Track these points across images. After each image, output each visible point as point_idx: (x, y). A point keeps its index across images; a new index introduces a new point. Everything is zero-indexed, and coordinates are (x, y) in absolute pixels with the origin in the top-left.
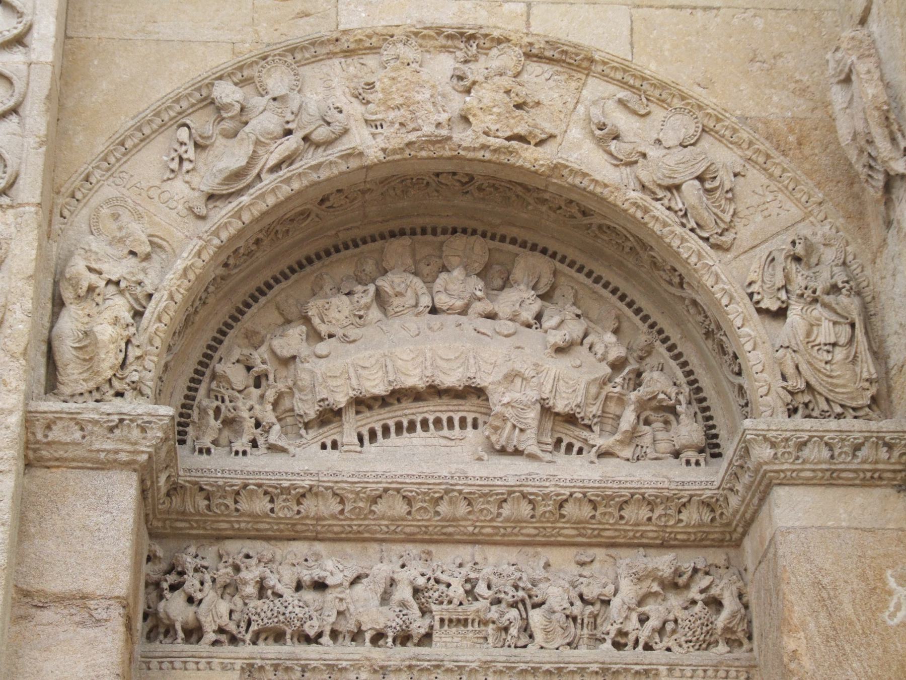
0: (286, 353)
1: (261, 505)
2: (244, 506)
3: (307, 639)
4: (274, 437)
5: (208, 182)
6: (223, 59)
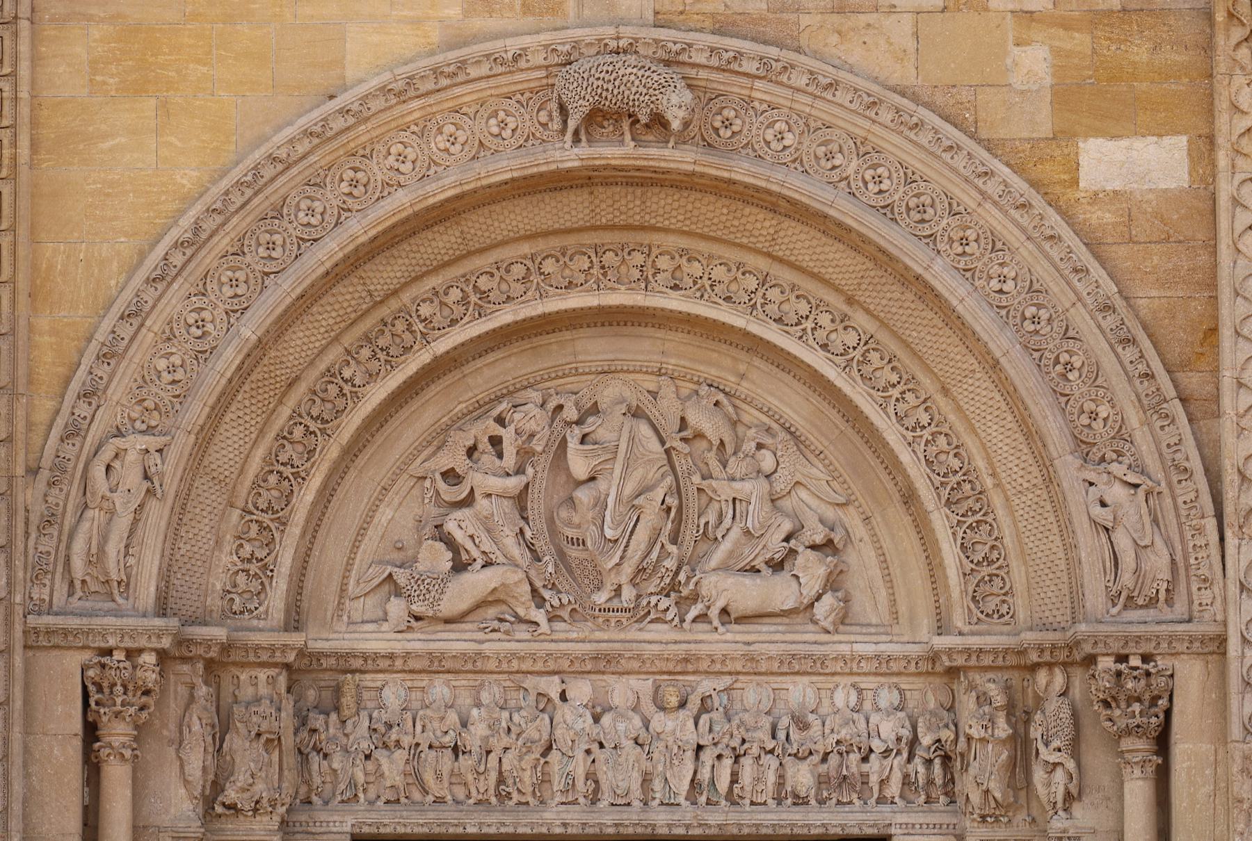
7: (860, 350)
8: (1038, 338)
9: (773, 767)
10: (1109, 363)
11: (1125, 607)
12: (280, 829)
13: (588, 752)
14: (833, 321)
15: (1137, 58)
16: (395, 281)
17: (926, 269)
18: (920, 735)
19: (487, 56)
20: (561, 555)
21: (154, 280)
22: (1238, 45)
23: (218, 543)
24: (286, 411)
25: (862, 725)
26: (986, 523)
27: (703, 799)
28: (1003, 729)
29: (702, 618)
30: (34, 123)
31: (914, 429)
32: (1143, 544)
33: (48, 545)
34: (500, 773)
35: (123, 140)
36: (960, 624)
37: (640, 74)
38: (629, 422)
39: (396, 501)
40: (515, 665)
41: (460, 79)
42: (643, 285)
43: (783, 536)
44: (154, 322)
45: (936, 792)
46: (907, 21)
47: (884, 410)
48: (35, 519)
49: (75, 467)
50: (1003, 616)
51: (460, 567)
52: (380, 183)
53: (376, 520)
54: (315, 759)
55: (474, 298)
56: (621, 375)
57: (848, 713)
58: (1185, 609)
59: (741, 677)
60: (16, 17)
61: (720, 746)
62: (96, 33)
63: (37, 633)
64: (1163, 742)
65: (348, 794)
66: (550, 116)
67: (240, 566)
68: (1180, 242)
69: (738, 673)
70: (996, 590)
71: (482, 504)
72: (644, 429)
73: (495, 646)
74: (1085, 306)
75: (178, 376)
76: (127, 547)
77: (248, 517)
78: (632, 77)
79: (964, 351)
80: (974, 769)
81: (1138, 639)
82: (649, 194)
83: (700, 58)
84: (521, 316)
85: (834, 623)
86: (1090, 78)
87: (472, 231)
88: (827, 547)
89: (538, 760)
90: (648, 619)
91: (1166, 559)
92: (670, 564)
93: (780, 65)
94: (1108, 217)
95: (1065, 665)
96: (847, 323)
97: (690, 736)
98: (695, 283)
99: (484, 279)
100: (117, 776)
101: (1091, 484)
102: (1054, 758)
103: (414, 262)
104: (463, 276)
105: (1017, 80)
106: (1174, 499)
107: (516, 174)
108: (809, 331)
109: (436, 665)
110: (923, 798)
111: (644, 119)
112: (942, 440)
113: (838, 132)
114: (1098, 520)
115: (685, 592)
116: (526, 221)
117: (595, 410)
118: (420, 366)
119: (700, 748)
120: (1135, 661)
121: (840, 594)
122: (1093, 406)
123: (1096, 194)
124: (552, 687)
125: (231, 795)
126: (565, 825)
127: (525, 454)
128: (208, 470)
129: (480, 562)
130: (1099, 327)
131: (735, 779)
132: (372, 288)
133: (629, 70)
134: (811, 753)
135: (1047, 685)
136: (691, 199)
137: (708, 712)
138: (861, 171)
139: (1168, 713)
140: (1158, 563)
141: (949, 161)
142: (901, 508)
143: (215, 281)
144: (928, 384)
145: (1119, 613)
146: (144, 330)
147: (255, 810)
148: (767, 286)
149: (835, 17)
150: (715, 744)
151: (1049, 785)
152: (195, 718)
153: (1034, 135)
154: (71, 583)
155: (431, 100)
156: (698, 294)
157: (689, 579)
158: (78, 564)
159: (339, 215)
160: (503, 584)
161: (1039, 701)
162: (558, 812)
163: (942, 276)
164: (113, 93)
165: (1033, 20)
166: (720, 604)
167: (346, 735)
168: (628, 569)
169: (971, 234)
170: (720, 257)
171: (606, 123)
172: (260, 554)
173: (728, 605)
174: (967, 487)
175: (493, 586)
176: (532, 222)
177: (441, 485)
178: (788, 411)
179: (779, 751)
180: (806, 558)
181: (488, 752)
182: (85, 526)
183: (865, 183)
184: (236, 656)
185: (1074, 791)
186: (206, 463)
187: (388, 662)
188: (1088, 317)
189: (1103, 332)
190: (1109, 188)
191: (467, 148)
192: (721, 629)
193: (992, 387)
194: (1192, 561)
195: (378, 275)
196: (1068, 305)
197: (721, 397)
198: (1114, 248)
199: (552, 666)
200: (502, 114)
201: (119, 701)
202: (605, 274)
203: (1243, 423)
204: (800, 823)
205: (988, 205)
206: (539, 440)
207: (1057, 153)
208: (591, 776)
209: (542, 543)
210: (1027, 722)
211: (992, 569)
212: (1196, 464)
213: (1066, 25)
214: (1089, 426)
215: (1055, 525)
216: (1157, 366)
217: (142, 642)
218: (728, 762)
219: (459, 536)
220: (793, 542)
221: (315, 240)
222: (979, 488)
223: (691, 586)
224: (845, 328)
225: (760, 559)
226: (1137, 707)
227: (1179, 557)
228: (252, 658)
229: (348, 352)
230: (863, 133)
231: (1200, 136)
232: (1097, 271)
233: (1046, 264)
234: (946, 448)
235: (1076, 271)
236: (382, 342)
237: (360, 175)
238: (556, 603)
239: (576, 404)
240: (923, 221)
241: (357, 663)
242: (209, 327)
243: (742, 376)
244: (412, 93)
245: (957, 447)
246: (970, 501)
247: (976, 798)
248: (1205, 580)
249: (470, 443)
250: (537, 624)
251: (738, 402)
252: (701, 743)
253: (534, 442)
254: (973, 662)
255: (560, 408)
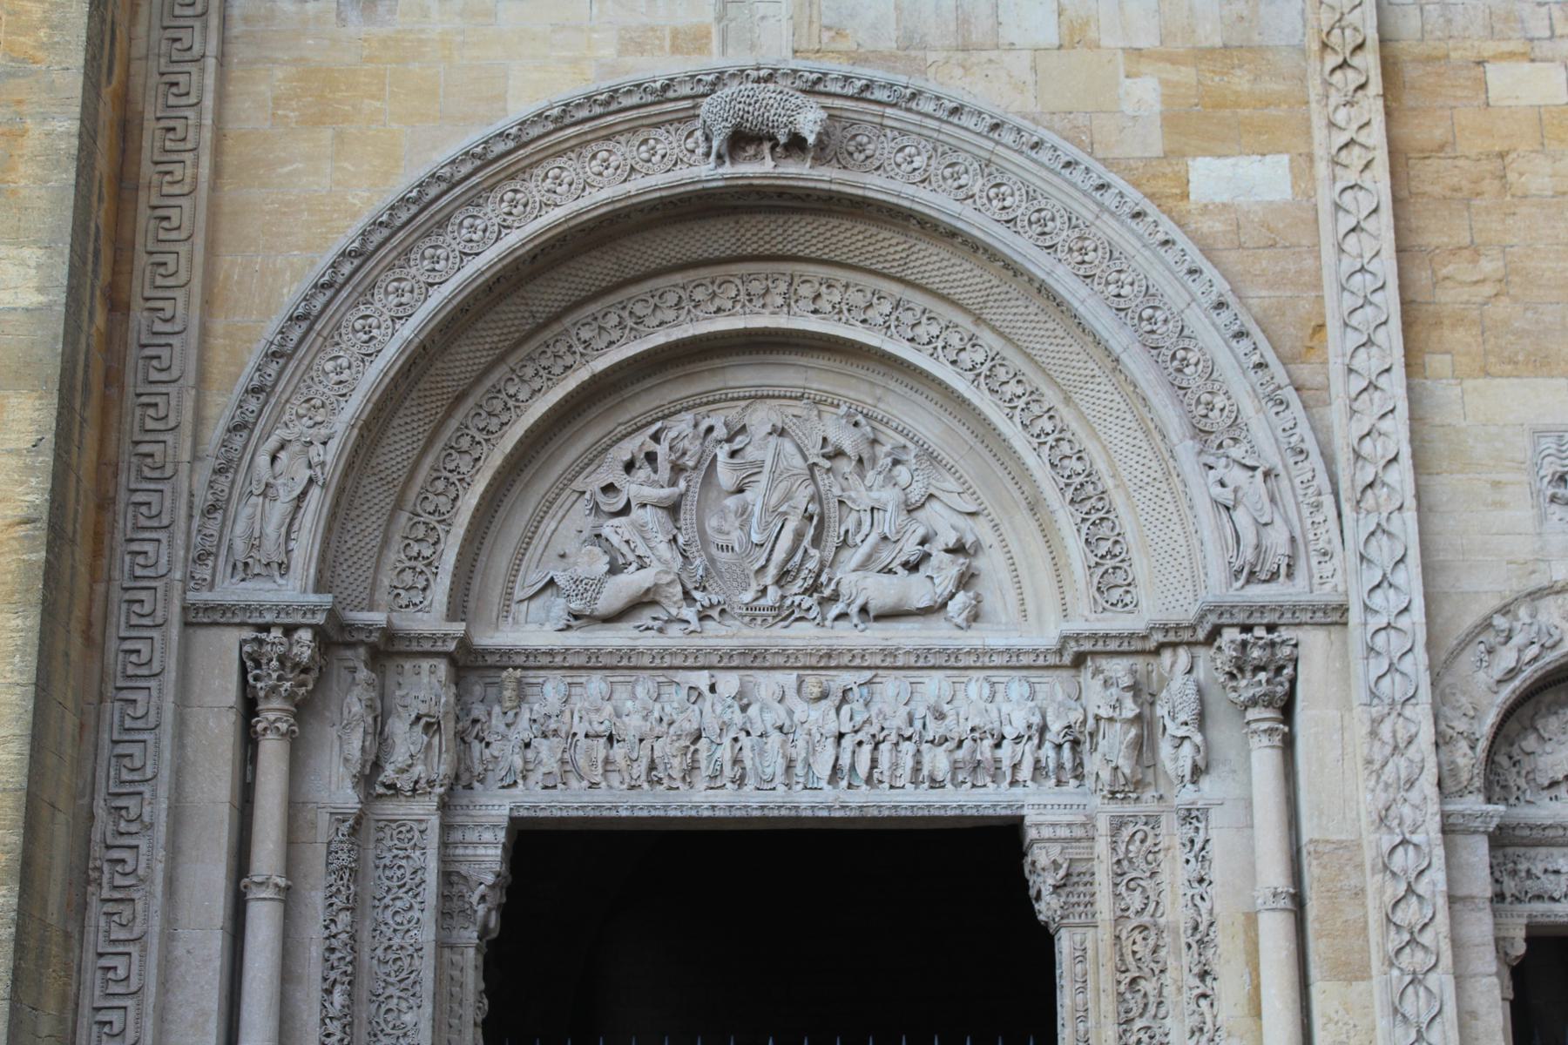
0: (1529, 750)
1: (1527, 832)
2: (1517, 832)
3: (1552, 899)
4: (1528, 797)
5: (1497, 673)
6: (1496, 603)
7: (988, 364)
8: (1155, 336)
9: (910, 754)
10: (1224, 359)
11: (1248, 582)
12: (438, 809)
13: (736, 740)
14: (961, 339)
15: (1239, 88)
16: (556, 304)
17: (1048, 274)
18: (1049, 723)
19: (639, 86)
20: (712, 560)
21: (322, 285)
22: (1333, 71)
23: (386, 543)
24: (454, 423)
25: (994, 715)
26: (1108, 519)
27: (844, 783)
28: (1130, 709)
29: (843, 616)
30: (217, 150)
31: (1039, 436)
32: (1263, 520)
33: (213, 527)
34: (653, 761)
35: (301, 165)
36: (1086, 613)
37: (778, 97)
38: (773, 439)
39: (560, 514)
40: (667, 661)
41: (614, 107)
42: (785, 309)
43: (918, 541)
44: (324, 327)
45: (1067, 775)
46: (1026, 57)
47: (1011, 418)
48: (199, 503)
49: (241, 458)
50: (1126, 605)
51: (614, 570)
52: (537, 205)
53: (540, 531)
54: (477, 747)
55: (630, 323)
56: (768, 401)
57: (982, 705)
58: (1306, 582)
59: (880, 672)
60: (203, 56)
61: (860, 734)
62: (279, 73)
63: (197, 610)
64: (1287, 710)
65: (508, 781)
66: (696, 143)
67: (408, 564)
68: (1286, 247)
69: (877, 668)
70: (1120, 582)
71: (636, 513)
72: (788, 446)
73: (651, 640)
74: (1199, 306)
75: (343, 377)
76: (288, 533)
77: (416, 519)
78: (772, 101)
79: (1083, 356)
80: (1103, 745)
81: (1262, 609)
82: (790, 223)
83: (834, 88)
84: (673, 338)
85: (967, 620)
86: (1196, 105)
87: (628, 258)
88: (958, 549)
89: (688, 747)
90: (793, 618)
91: (1286, 536)
92: (812, 564)
93: (908, 92)
94: (1219, 227)
95: (1189, 644)
96: (974, 341)
97: (832, 727)
98: (834, 307)
99: (640, 305)
100: (272, 753)
101: (1211, 468)
102: (1182, 732)
103: (573, 286)
104: (621, 303)
105: (1129, 108)
106: (1291, 480)
107: (664, 193)
108: (939, 349)
109: (593, 662)
110: (1053, 781)
111: (783, 139)
112: (1065, 448)
113: (963, 155)
114: (1220, 500)
115: (827, 592)
116: (677, 249)
117: (743, 429)
118: (579, 382)
119: (841, 736)
120: (1260, 632)
121: (971, 594)
122: (1208, 397)
123: (1206, 206)
124: (702, 679)
125: (389, 773)
126: (713, 807)
127: (677, 469)
128: (376, 470)
129: (634, 566)
130: (1213, 324)
131: (874, 763)
132: (534, 309)
133: (769, 95)
134: (946, 740)
135: (1172, 666)
136: (829, 226)
137: (847, 702)
138: (986, 188)
139: (1293, 682)
140: (1277, 540)
141: (1068, 176)
142: (1026, 513)
143: (382, 290)
144: (1051, 397)
145: (1243, 587)
146: (313, 335)
147: (414, 790)
148: (900, 309)
149: (960, 55)
150: (856, 732)
151: (1176, 759)
152: (355, 700)
153: (1146, 155)
154: (234, 566)
155: (587, 127)
156: (836, 317)
157: (830, 580)
158: (239, 545)
159: (500, 232)
160: (656, 585)
161: (1164, 682)
162: (707, 797)
163: (1064, 280)
164: (293, 125)
165: (1141, 56)
166: (859, 602)
167: (508, 725)
168: (772, 571)
169: (1089, 245)
170: (856, 285)
171: (748, 148)
172: (427, 552)
173: (866, 603)
174: (1090, 488)
175: (647, 585)
176: (683, 251)
177: (601, 498)
178: (921, 429)
179: (916, 738)
180: (939, 557)
181: (641, 741)
182: (248, 511)
183: (990, 200)
184: (402, 647)
185: (1202, 764)
186: (373, 462)
187: (549, 659)
188: (1202, 316)
189: (1218, 330)
190: (1218, 200)
191: (619, 171)
192: (861, 626)
193: (1111, 389)
194: (1311, 537)
195: (540, 296)
196: (1183, 306)
197: (859, 418)
198: (1225, 253)
199: (701, 661)
200: (652, 142)
201: (275, 675)
202: (750, 301)
203: (1356, 406)
204: (937, 805)
205: (1106, 216)
206: (691, 457)
207: (1168, 170)
208: (736, 761)
209: (694, 549)
210: (1152, 704)
211: (1115, 562)
212: (1311, 445)
213: (1173, 59)
214: (1206, 416)
215: (1175, 514)
216: (1271, 357)
217: (297, 618)
218: (867, 748)
219: (615, 540)
220: (927, 547)
221: (477, 254)
222: (1100, 488)
223: (832, 586)
224: (973, 346)
225: (897, 561)
226: (1262, 676)
227: (1298, 534)
228: (415, 647)
229: (513, 371)
230: (987, 155)
231: (1300, 155)
232: (1209, 271)
233: (1161, 268)
234: (1068, 452)
235: (1191, 272)
236: (544, 363)
237: (519, 196)
238: (706, 603)
239: (726, 424)
240: (1044, 234)
241: (520, 660)
242: (375, 332)
243: (879, 399)
244: (567, 120)
245: (1080, 451)
246: (1093, 500)
247: (1106, 775)
248: (1325, 554)
249: (627, 457)
250: (688, 622)
251: (876, 424)
252: (843, 731)
253: (687, 457)
254: (1100, 647)
255: (710, 429)
